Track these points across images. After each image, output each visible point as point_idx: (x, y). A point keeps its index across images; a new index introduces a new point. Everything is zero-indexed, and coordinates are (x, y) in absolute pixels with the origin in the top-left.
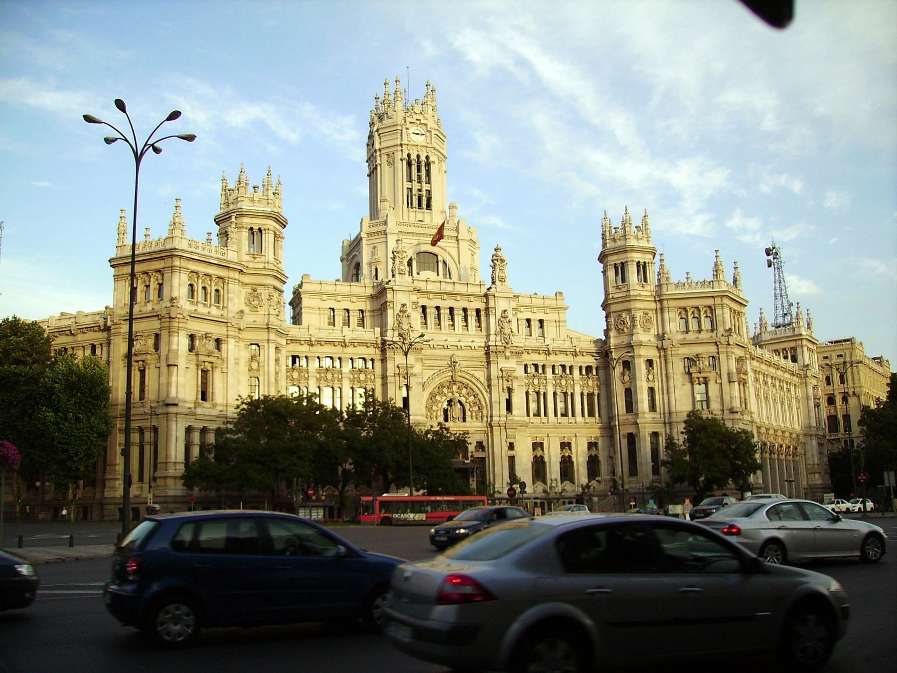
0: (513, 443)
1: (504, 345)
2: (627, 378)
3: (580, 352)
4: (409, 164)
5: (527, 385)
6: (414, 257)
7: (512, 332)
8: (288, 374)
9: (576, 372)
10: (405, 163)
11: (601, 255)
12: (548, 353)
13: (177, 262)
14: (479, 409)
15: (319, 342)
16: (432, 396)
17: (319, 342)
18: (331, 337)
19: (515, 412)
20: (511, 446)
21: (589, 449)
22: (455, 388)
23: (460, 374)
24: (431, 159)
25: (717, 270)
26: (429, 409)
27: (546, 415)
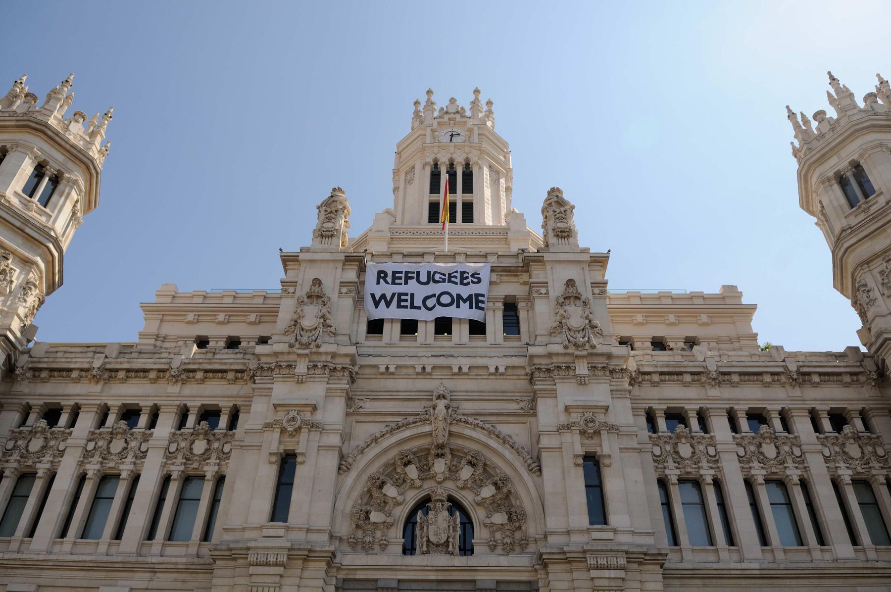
1: (570, 351)
3: (799, 373)
7: (593, 327)
8: (20, 442)
11: (803, 208)
14: (510, 519)
15: (109, 374)
19: (617, 518)
22: (440, 466)
23: (454, 429)
27: (731, 540)
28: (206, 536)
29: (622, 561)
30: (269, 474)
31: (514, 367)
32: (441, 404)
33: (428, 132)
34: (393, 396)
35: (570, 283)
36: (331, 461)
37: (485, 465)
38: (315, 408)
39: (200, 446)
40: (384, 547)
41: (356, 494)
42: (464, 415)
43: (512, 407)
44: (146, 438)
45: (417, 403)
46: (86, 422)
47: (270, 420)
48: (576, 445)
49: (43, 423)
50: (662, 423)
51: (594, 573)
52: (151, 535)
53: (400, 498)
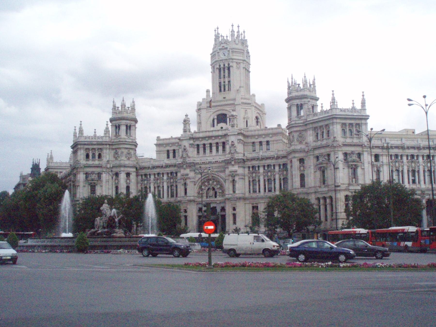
3: (277, 157)
4: (220, 70)
5: (249, 178)
6: (216, 117)
9: (277, 168)
10: (218, 71)
13: (79, 146)
16: (200, 188)
17: (154, 167)
19: (237, 192)
20: (234, 209)
22: (211, 182)
23: (212, 175)
24: (231, 64)
25: (333, 101)
26: (199, 193)
28: (177, 196)
30: (183, 188)
31: (223, 161)
33: (217, 54)
41: (198, 188)
42: (214, 172)
43: (223, 169)
44: (163, 179)
46: (152, 177)
47: (182, 177)
48: (231, 179)
49: (145, 178)
52: (168, 197)
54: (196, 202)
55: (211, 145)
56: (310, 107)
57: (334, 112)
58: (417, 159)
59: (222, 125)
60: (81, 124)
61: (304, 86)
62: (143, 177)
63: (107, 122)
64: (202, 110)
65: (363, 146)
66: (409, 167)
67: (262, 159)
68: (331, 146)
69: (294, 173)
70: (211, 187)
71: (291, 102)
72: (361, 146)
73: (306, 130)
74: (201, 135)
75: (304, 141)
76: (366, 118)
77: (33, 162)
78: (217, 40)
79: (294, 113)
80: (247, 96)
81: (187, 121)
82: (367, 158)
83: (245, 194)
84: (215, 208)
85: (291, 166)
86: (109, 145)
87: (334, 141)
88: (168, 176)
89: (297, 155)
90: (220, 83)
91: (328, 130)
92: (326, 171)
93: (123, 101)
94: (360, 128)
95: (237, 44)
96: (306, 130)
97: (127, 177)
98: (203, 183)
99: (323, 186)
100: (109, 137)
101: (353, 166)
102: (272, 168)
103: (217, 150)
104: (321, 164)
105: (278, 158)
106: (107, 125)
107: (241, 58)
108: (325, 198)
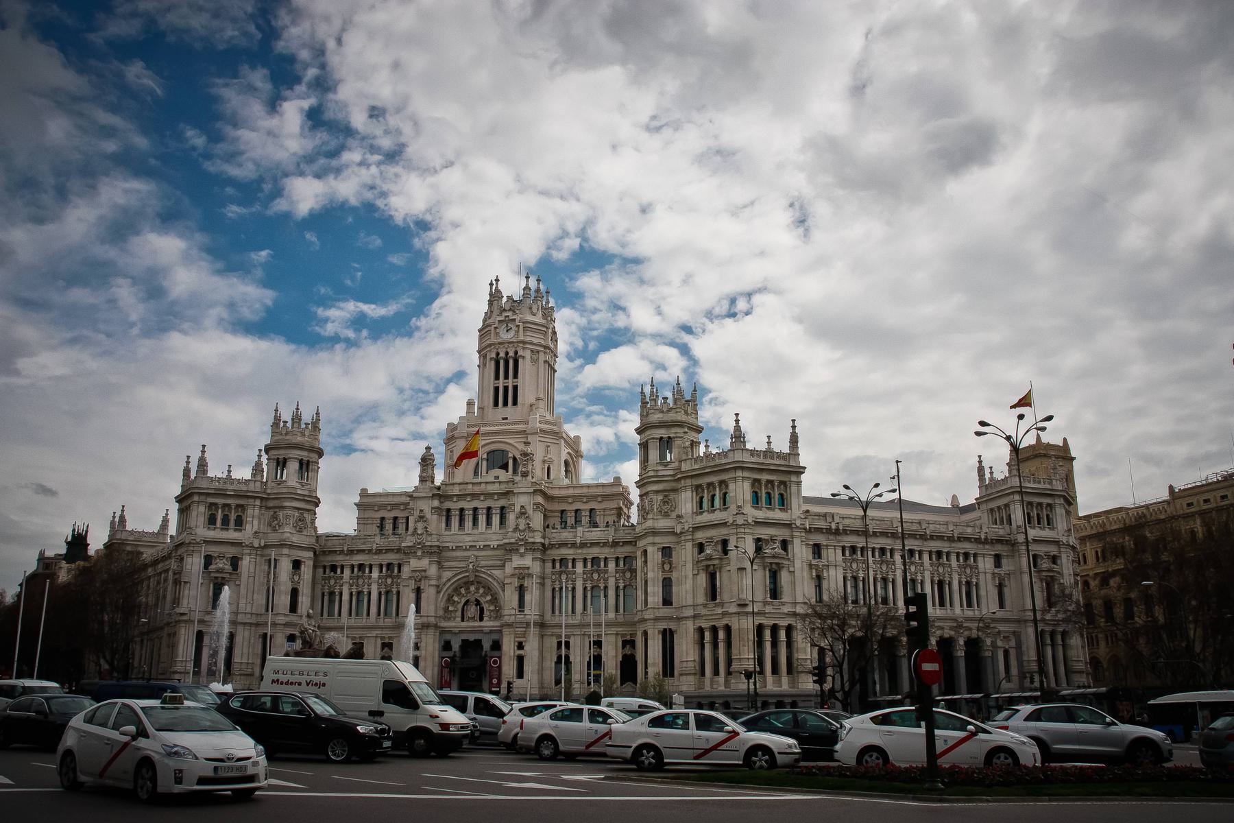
0: (522, 642)
2: (645, 569)
3: (613, 542)
7: (529, 528)
9: (612, 565)
10: (493, 362)
12: (574, 545)
13: (196, 498)
15: (351, 552)
16: (450, 599)
18: (363, 547)
19: (526, 612)
20: (520, 646)
21: (623, 648)
22: (472, 588)
23: (477, 574)
24: (519, 354)
26: (446, 610)
28: (397, 614)
29: (525, 626)
30: (413, 596)
31: (501, 545)
32: (471, 567)
33: (493, 329)
34: (455, 559)
35: (522, 506)
36: (432, 591)
37: (489, 588)
38: (425, 571)
39: (389, 581)
40: (455, 619)
42: (481, 567)
44: (370, 578)
45: (464, 562)
46: (347, 572)
48: (516, 583)
50: (558, 565)
51: (517, 629)
52: (379, 615)
53: (459, 601)
54: (440, 627)
55: (475, 509)
56: (688, 444)
57: (738, 456)
58: (891, 557)
59: (500, 472)
60: (203, 452)
61: (675, 401)
62: (328, 571)
63: (260, 450)
64: (458, 441)
65: (793, 526)
66: (876, 571)
67: (583, 545)
68: (732, 524)
69: (650, 575)
70: (473, 599)
71: (648, 433)
72: (789, 526)
73: (677, 490)
74: (456, 490)
75: (672, 511)
76: (800, 471)
77: (74, 530)
78: (495, 303)
79: (654, 455)
80: (548, 417)
81: (431, 459)
82: (800, 552)
83: (542, 616)
84: (478, 644)
85: (646, 562)
86: (262, 499)
87: (737, 514)
88: (381, 571)
89: (658, 539)
90: (497, 389)
91: (724, 491)
92: (718, 574)
93: (297, 409)
94: (786, 491)
95: (535, 315)
96: (675, 490)
97: (294, 567)
98: (456, 590)
99: (711, 604)
100: (262, 482)
101: (774, 566)
102: (602, 564)
103: (489, 523)
104: (710, 558)
105: (615, 544)
106: (260, 456)
107: (542, 342)
108: (714, 630)
